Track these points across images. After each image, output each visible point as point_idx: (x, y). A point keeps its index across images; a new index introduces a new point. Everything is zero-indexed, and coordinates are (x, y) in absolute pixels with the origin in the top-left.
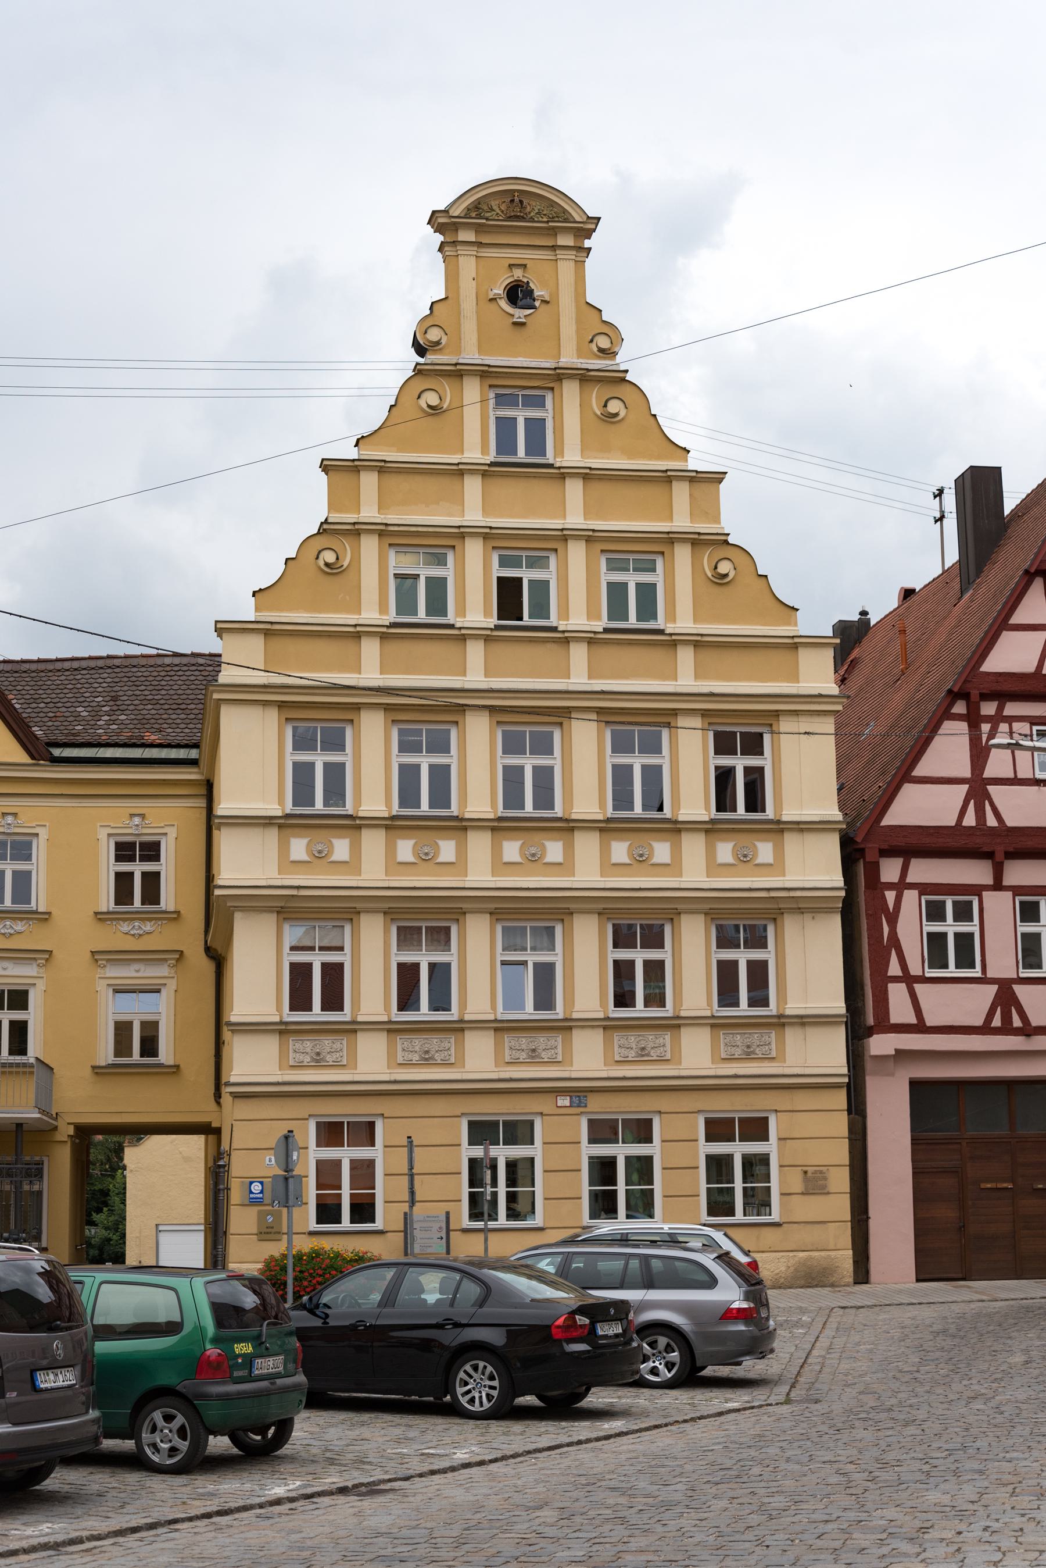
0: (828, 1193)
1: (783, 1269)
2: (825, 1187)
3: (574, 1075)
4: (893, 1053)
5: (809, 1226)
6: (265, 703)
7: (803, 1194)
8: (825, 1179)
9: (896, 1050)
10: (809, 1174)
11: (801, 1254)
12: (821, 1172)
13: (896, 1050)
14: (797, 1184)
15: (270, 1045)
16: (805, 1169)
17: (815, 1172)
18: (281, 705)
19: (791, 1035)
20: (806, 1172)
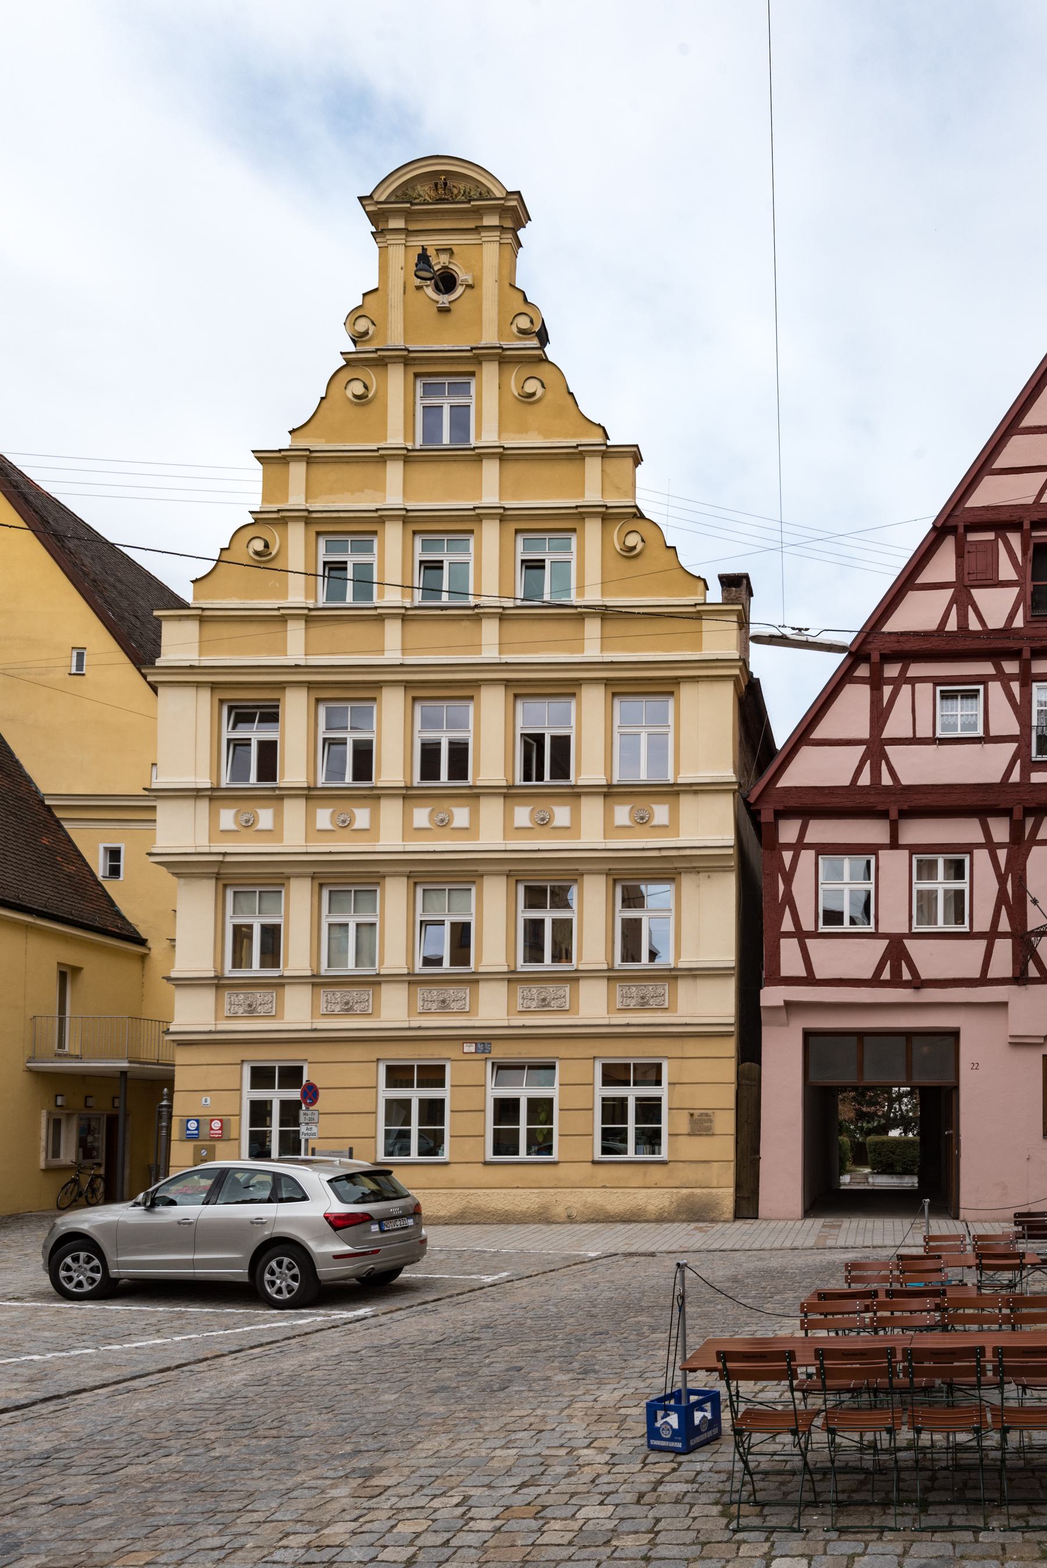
0: (713, 1135)
1: (667, 1204)
2: (709, 1129)
3: (478, 1024)
4: (782, 1004)
5: (694, 1165)
6: (198, 685)
7: (689, 1135)
8: (711, 1121)
9: (785, 1001)
10: (696, 1117)
11: (684, 1191)
12: (707, 1115)
13: (785, 1001)
14: (684, 1126)
15: (207, 998)
16: (692, 1111)
17: (701, 1115)
18: (214, 686)
19: (684, 987)
20: (692, 1115)
